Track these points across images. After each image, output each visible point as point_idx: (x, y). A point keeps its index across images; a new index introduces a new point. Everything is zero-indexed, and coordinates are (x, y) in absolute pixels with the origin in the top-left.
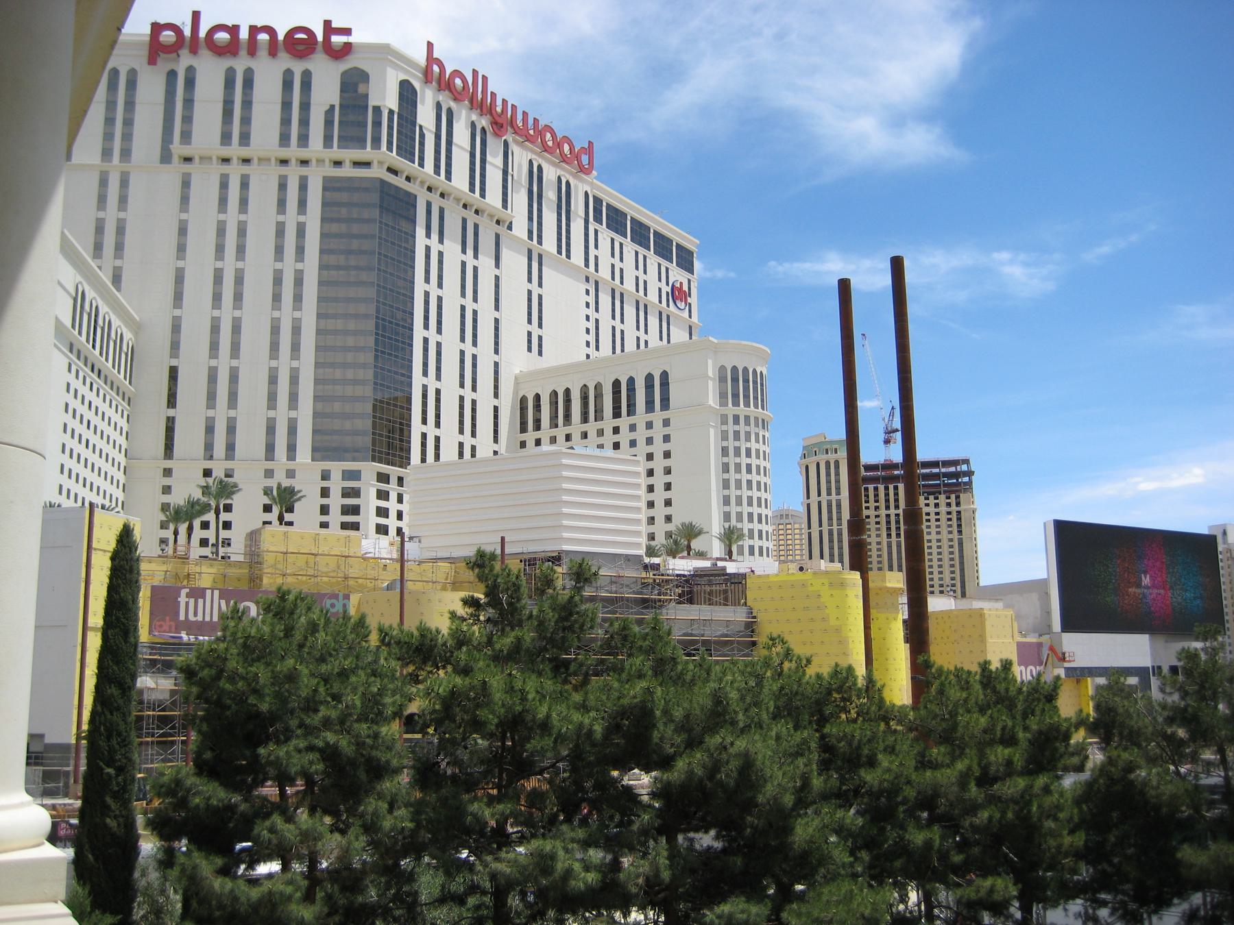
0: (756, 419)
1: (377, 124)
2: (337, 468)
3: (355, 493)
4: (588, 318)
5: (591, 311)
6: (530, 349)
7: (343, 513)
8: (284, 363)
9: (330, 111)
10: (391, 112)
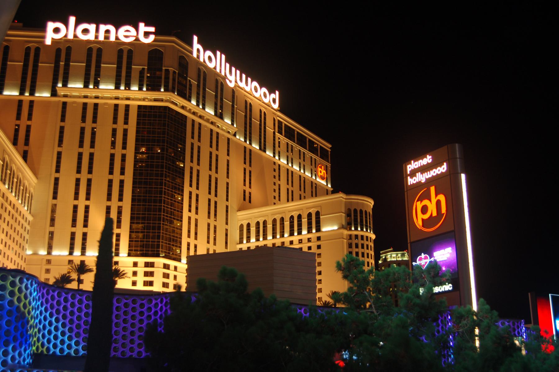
0: (367, 237)
1: (167, 78)
2: (141, 260)
3: (151, 274)
4: (275, 184)
5: (276, 180)
6: (244, 199)
7: (144, 285)
8: (114, 204)
9: (142, 72)
10: (174, 72)
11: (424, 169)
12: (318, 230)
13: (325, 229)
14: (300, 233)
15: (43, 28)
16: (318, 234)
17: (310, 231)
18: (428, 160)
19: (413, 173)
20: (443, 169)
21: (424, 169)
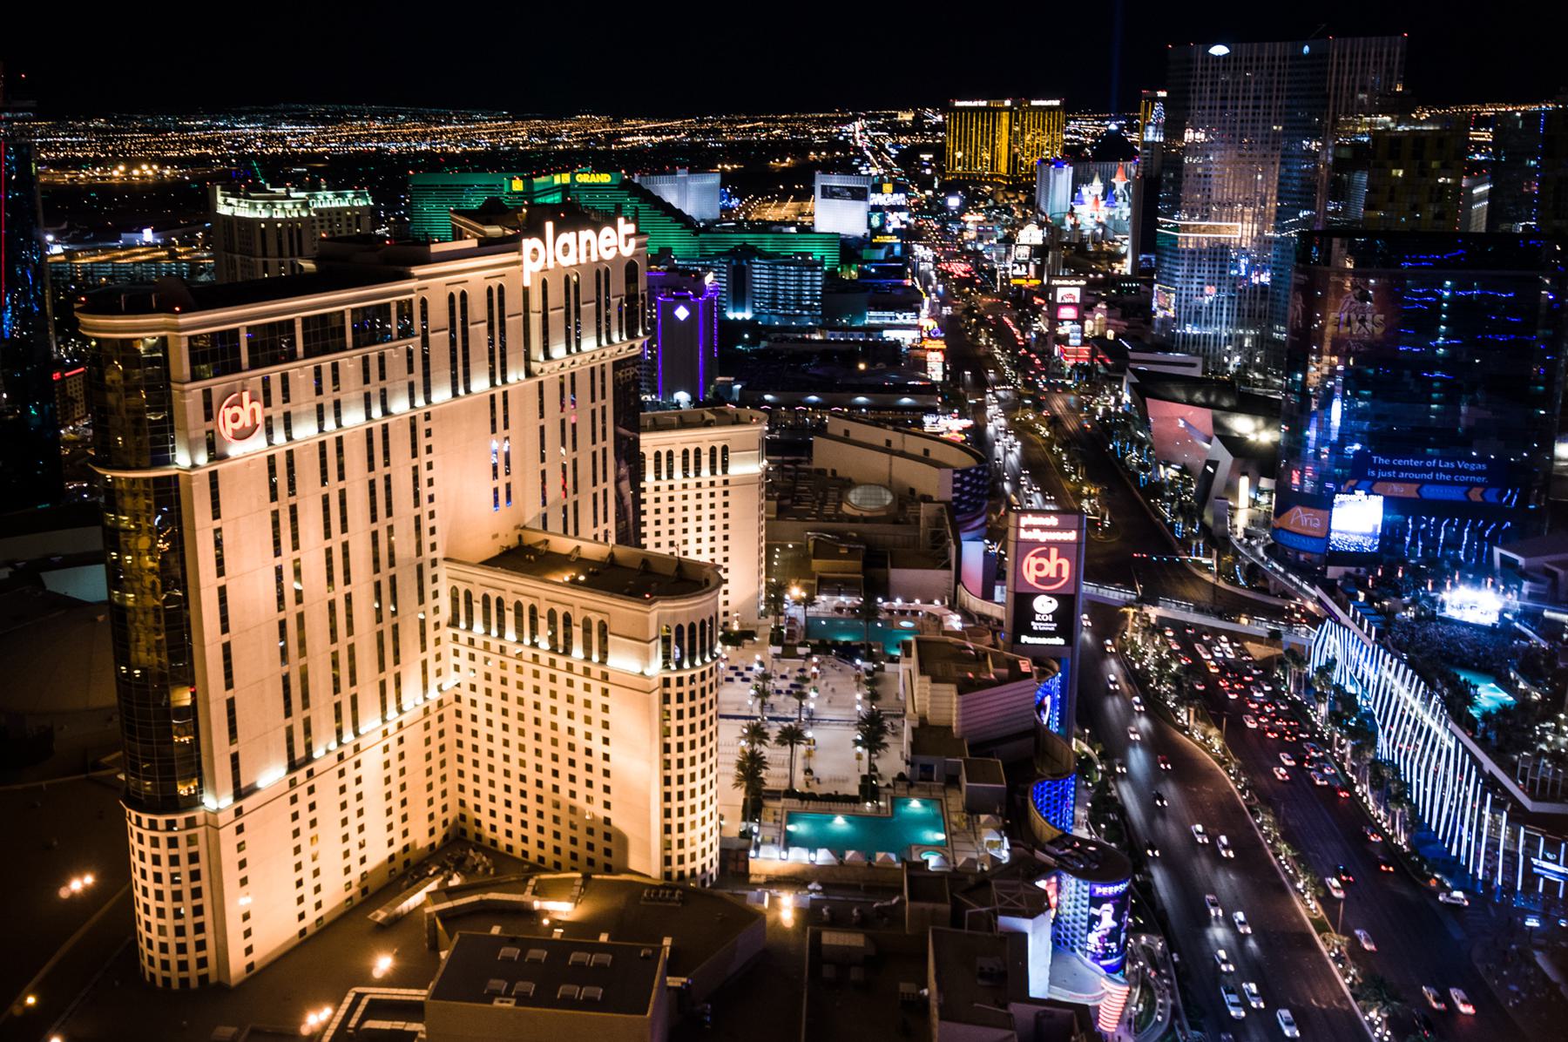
11: (1043, 528)
12: (725, 471)
13: (733, 470)
14: (697, 474)
15: (518, 249)
16: (725, 477)
17: (713, 472)
18: (1053, 521)
19: (1029, 528)
20: (1072, 536)
21: (1043, 528)
